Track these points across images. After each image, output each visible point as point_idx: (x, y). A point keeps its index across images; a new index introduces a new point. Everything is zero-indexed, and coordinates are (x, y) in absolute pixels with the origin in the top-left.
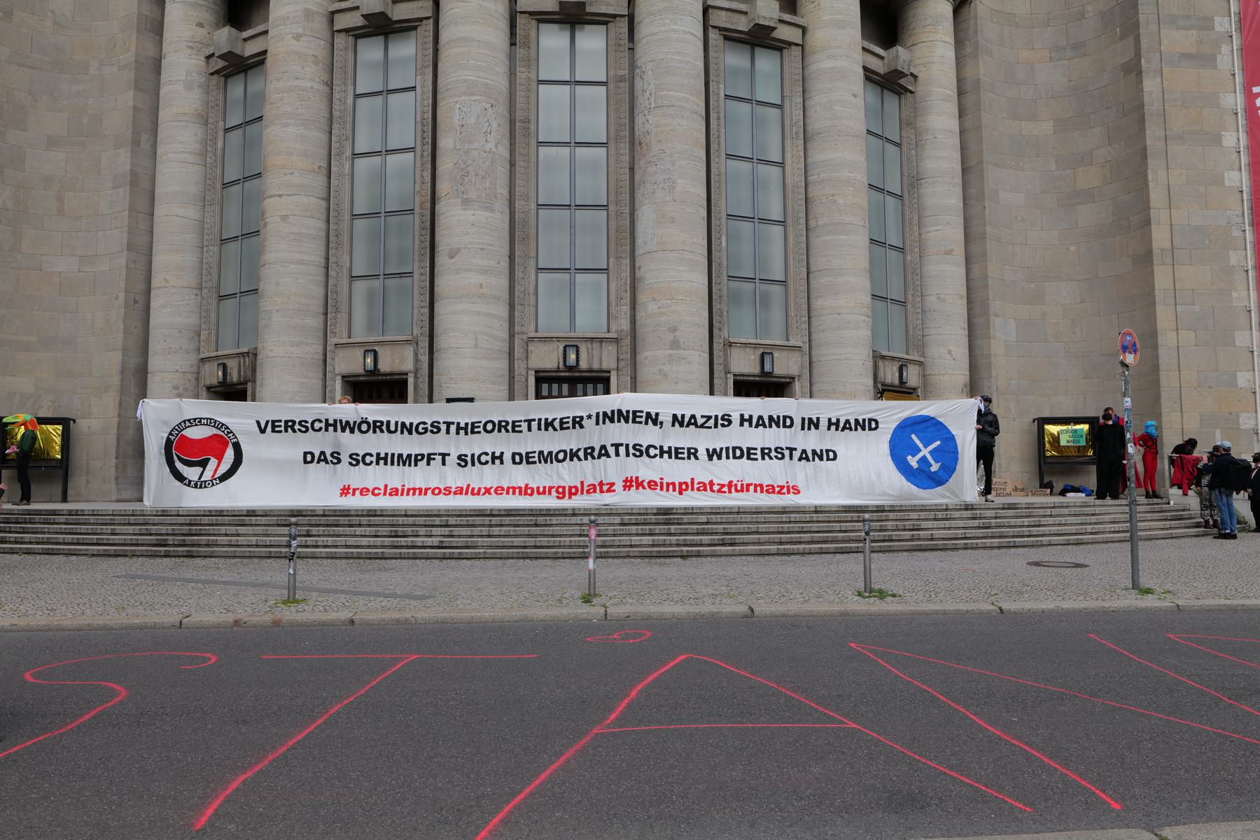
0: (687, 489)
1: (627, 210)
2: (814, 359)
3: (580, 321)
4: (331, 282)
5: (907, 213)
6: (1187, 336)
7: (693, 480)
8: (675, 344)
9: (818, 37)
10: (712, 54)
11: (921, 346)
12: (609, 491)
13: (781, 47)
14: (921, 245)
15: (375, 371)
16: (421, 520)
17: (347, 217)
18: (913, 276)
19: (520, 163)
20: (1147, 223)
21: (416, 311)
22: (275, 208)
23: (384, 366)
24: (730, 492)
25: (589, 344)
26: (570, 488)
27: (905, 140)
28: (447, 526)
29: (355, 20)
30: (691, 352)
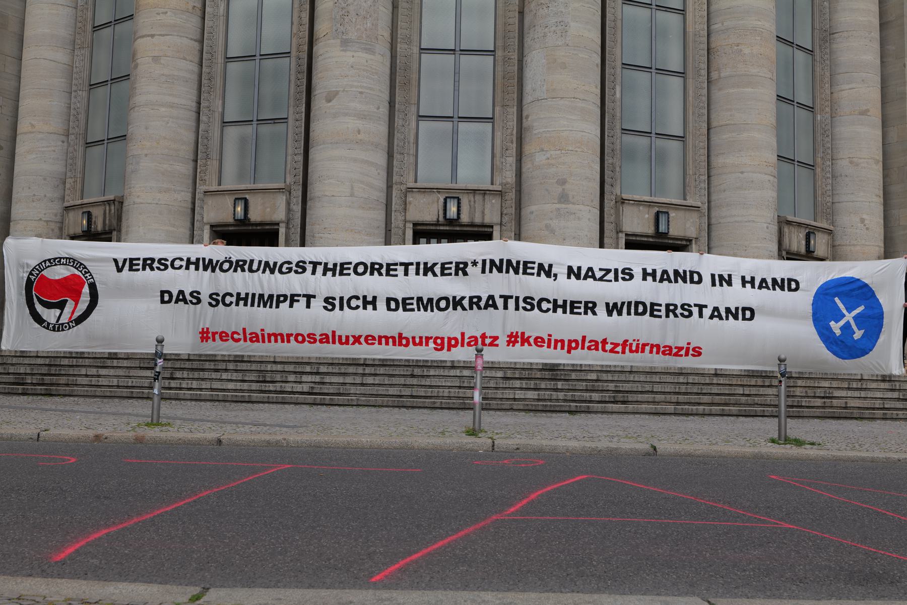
0: (576, 348)
1: (515, 56)
2: (713, 221)
3: (462, 173)
4: (202, 127)
5: (818, 69)
7: (584, 338)
8: (564, 198)
11: (831, 212)
12: (491, 344)
14: (833, 104)
15: (245, 221)
16: (291, 368)
17: (220, 59)
18: (823, 138)
21: (289, 158)
22: (146, 47)
23: (255, 216)
24: (623, 352)
25: (471, 196)
26: (450, 339)
28: (317, 373)
30: (581, 207)
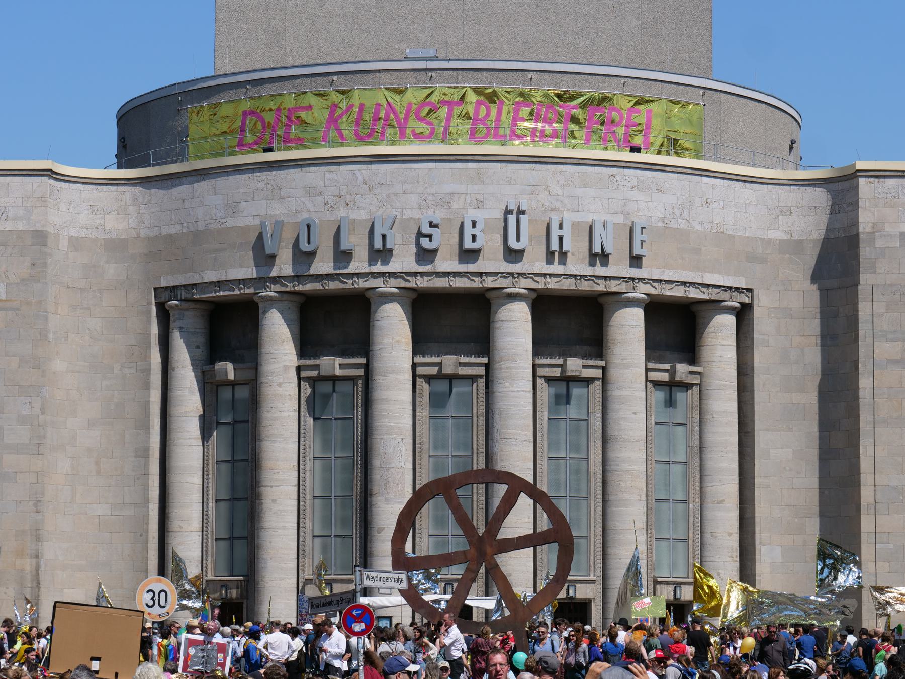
9: (613, 373)
10: (538, 393)
13: (588, 381)
19: (418, 470)
20: (857, 485)
27: (690, 420)
29: (314, 373)
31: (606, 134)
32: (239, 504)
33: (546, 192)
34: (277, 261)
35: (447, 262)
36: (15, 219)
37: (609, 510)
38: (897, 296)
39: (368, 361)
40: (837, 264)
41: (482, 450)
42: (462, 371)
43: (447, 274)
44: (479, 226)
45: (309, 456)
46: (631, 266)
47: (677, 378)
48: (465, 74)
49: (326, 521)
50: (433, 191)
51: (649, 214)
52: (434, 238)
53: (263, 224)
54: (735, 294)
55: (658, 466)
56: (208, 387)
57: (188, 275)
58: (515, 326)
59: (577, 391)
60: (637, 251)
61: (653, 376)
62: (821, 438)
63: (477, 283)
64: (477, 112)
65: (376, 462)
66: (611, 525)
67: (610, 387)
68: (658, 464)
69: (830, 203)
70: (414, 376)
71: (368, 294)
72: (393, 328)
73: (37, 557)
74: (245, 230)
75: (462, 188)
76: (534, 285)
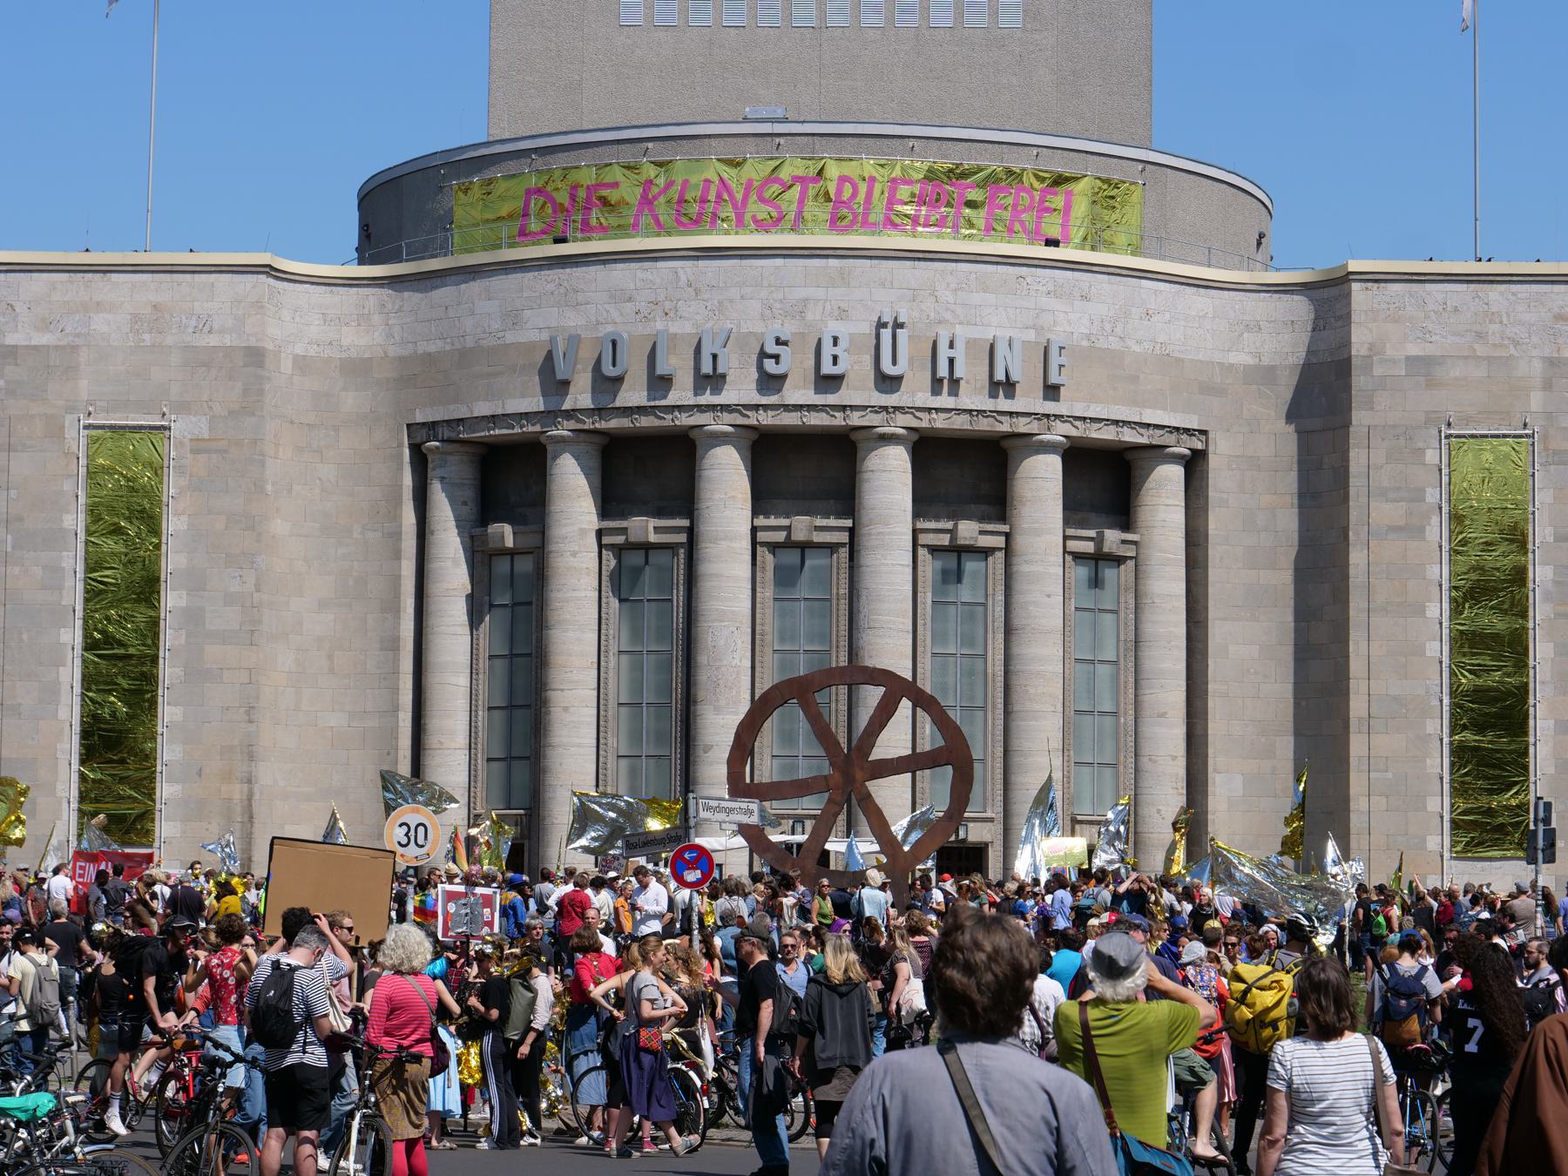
6: (1379, 802)
9: (1020, 542)
10: (920, 568)
13: (986, 552)
19: (758, 669)
27: (1122, 605)
29: (620, 539)
31: (1012, 221)
32: (519, 713)
33: (932, 299)
34: (572, 389)
35: (799, 392)
36: (222, 331)
37: (1013, 725)
38: (1402, 441)
39: (692, 523)
40: (1322, 398)
41: (844, 643)
42: (819, 537)
43: (798, 408)
44: (842, 343)
45: (613, 649)
46: (1045, 398)
47: (1106, 550)
48: (824, 140)
49: (635, 736)
50: (780, 296)
51: (1069, 329)
52: (782, 359)
53: (552, 340)
54: (1184, 437)
55: (1079, 666)
56: (478, 557)
57: (452, 407)
58: (889, 478)
59: (971, 565)
60: (1054, 379)
61: (1074, 546)
62: (1296, 631)
63: (838, 420)
64: (839, 191)
65: (702, 659)
66: (1015, 744)
67: (1016, 560)
68: (1080, 663)
69: (1312, 316)
70: (754, 543)
71: (693, 434)
72: (726, 479)
73: (249, 781)
74: (531, 346)
75: (820, 293)
76: (915, 423)
